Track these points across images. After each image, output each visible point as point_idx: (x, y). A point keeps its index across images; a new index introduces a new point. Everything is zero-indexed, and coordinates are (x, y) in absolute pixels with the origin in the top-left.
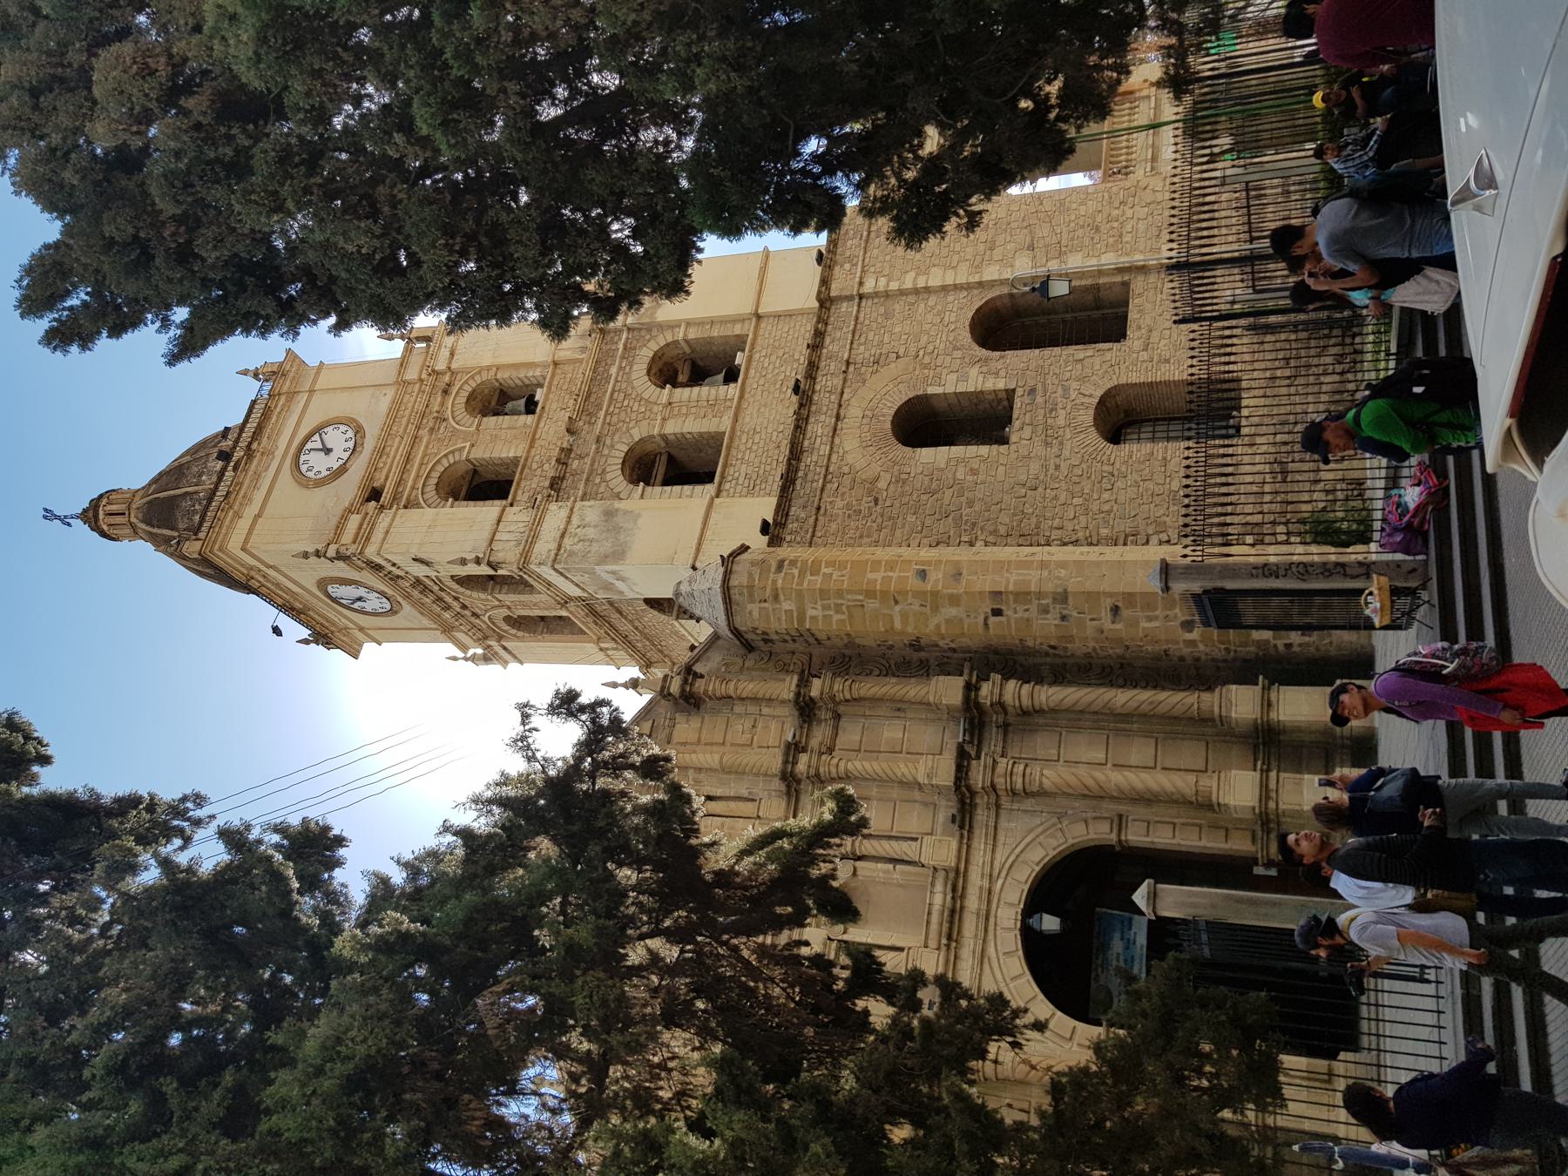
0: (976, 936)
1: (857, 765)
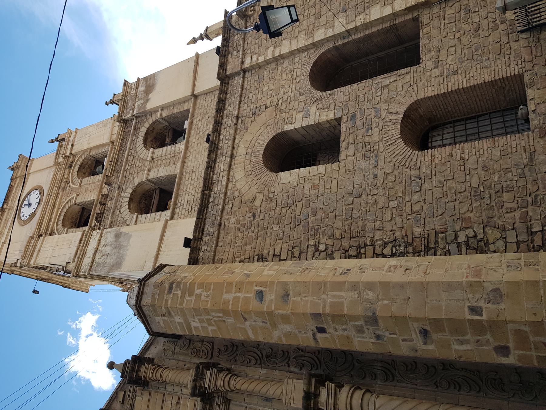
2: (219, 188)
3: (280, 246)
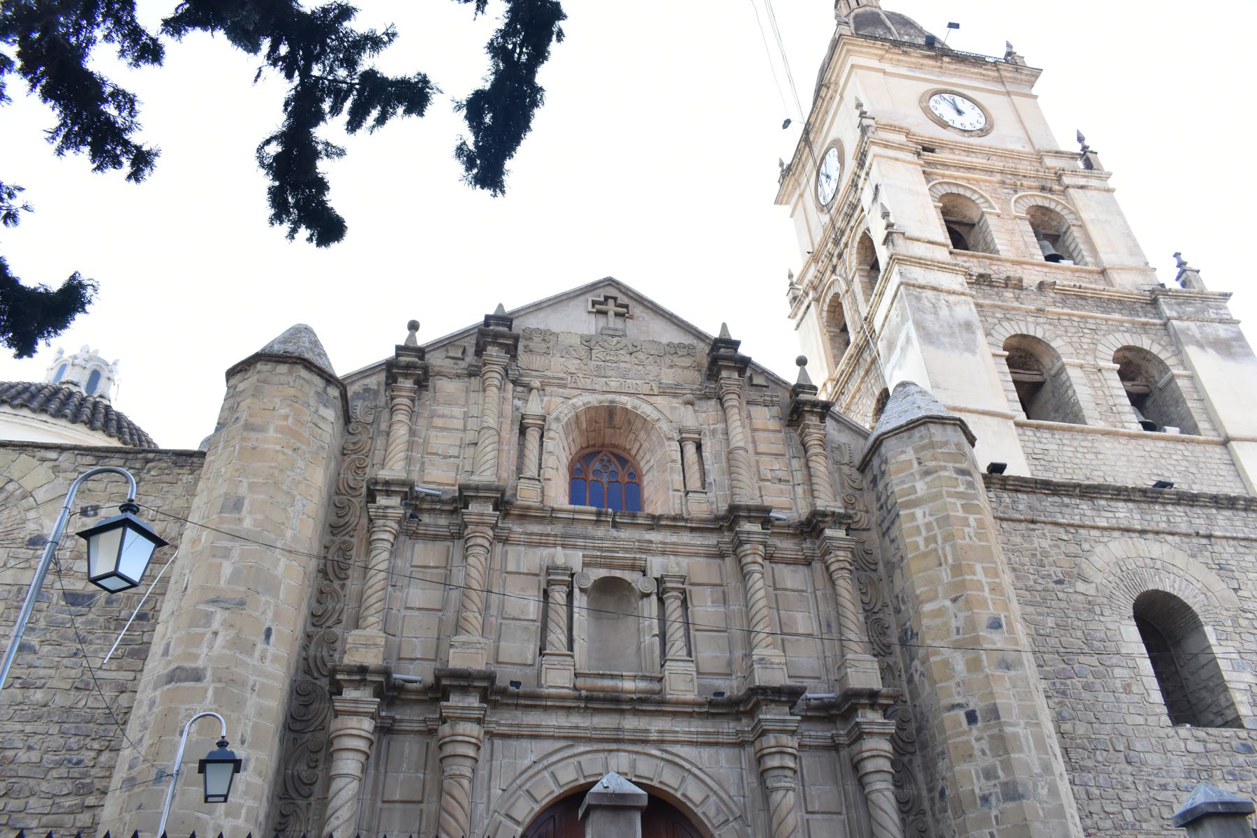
0: (595, 729)
1: (758, 583)
2: (1089, 513)
3: (1029, 632)
